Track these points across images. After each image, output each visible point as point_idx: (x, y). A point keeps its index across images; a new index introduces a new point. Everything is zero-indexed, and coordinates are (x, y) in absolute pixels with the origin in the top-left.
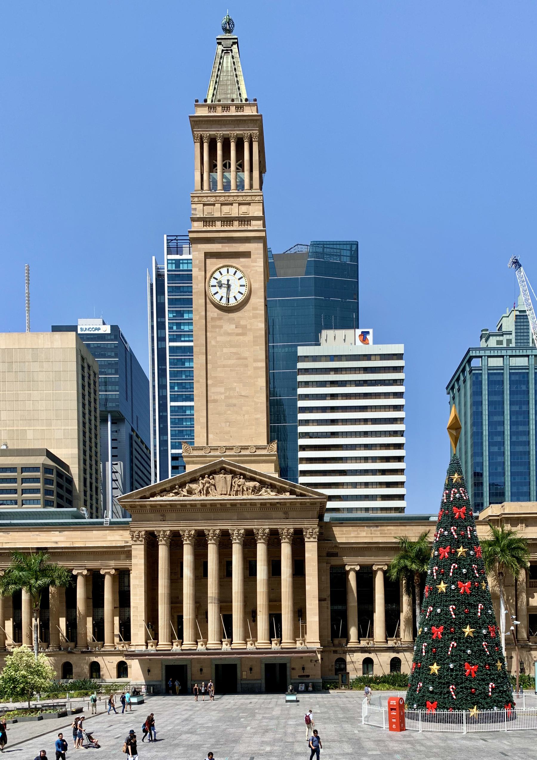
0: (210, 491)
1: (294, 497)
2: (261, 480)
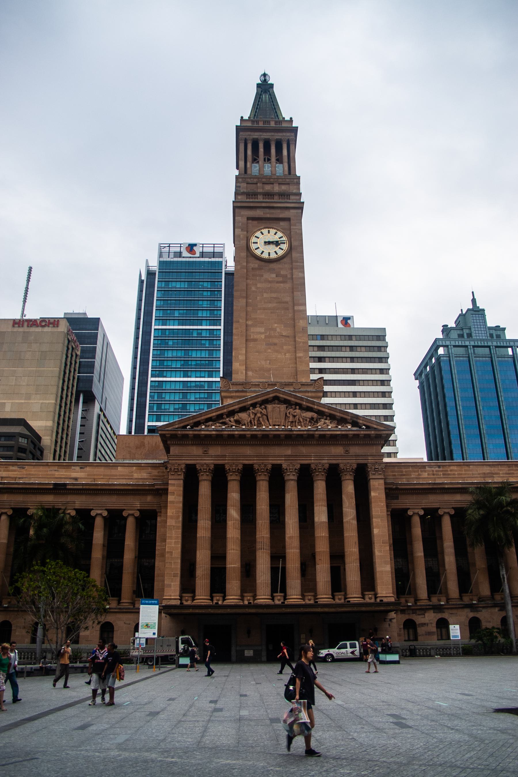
0: (262, 421)
1: (358, 429)
2: (319, 410)
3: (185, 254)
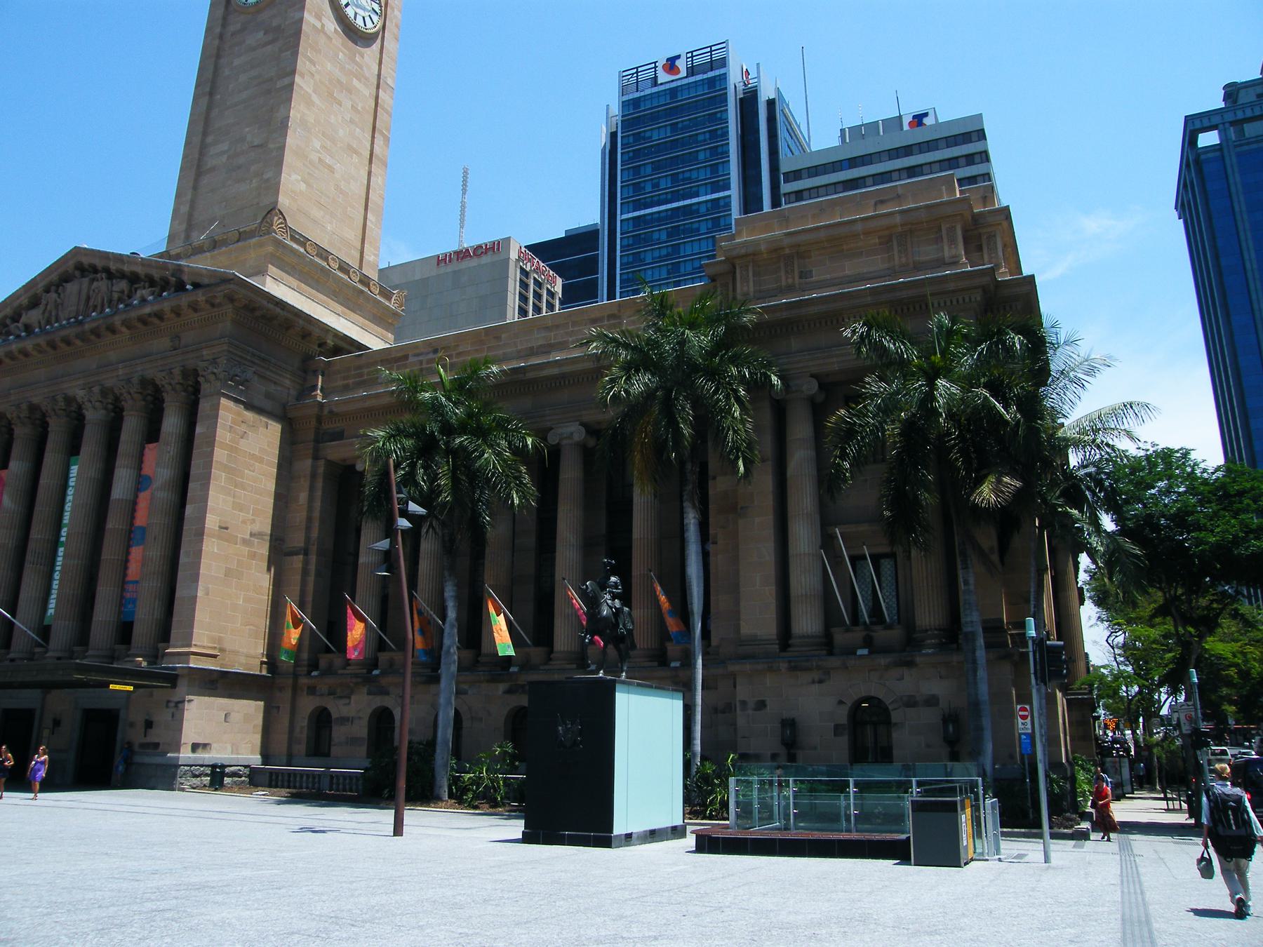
3: (663, 77)
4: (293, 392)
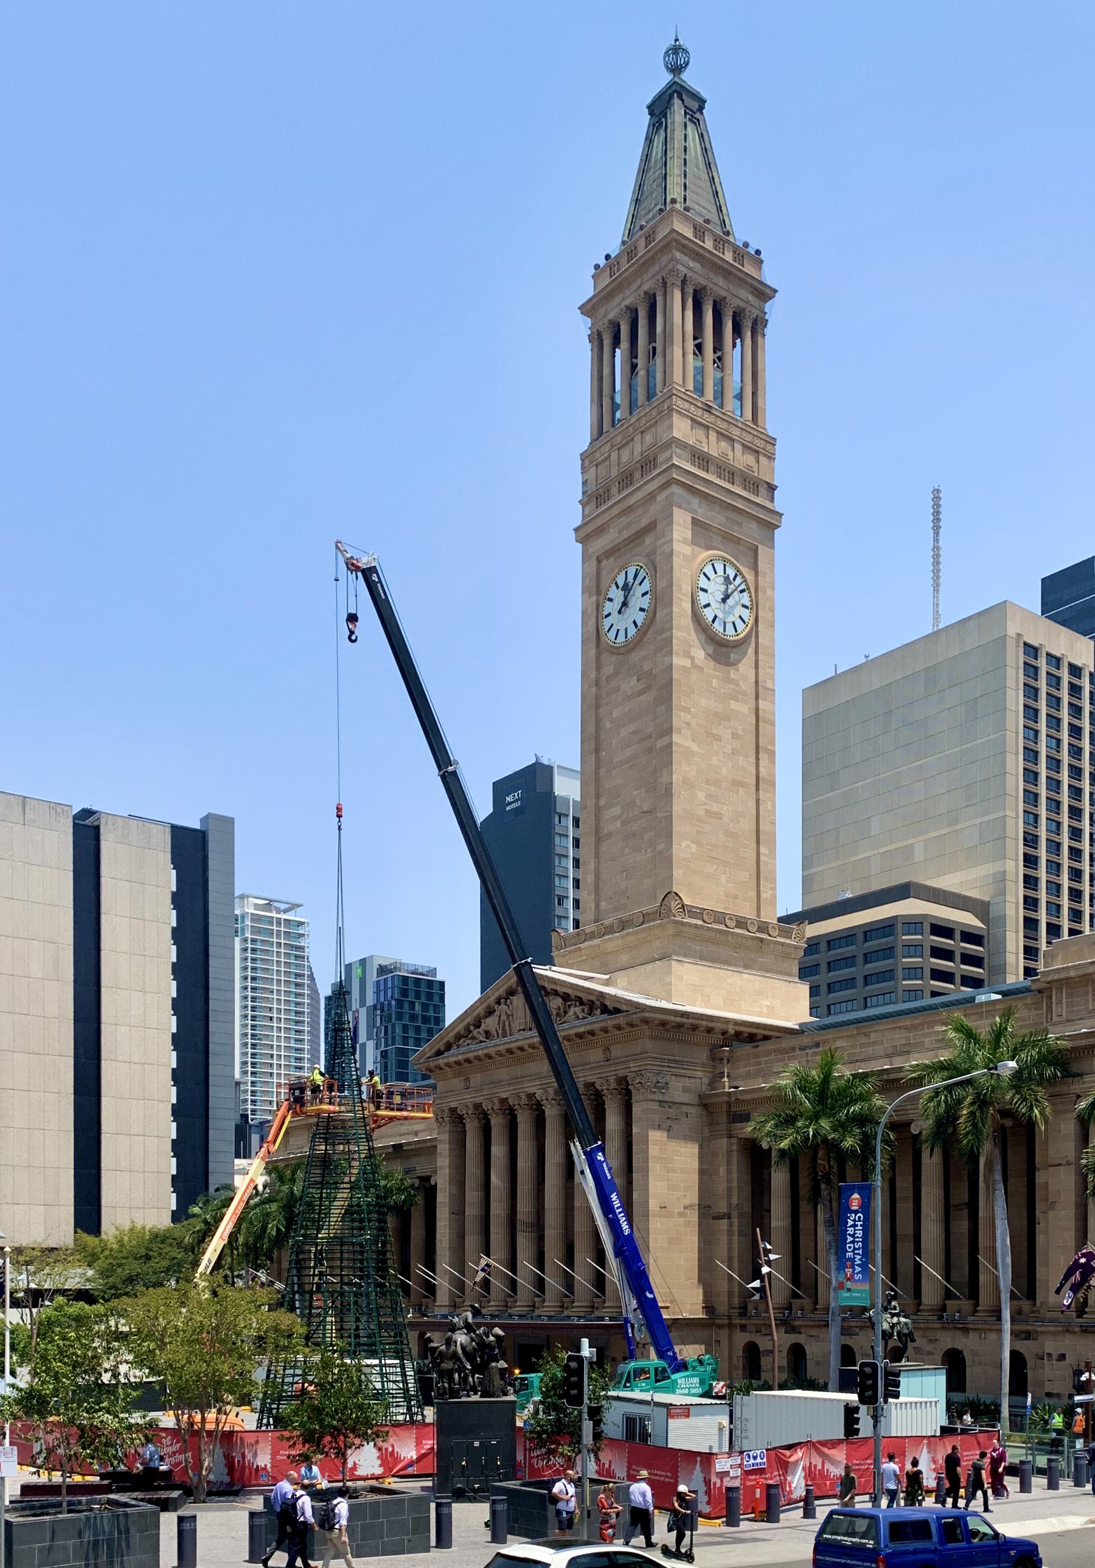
4: (706, 1081)
